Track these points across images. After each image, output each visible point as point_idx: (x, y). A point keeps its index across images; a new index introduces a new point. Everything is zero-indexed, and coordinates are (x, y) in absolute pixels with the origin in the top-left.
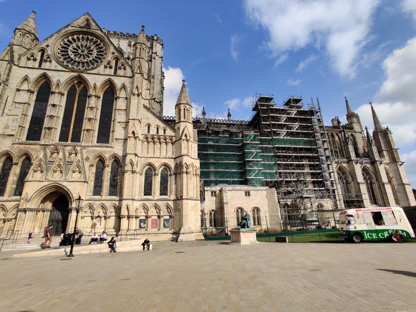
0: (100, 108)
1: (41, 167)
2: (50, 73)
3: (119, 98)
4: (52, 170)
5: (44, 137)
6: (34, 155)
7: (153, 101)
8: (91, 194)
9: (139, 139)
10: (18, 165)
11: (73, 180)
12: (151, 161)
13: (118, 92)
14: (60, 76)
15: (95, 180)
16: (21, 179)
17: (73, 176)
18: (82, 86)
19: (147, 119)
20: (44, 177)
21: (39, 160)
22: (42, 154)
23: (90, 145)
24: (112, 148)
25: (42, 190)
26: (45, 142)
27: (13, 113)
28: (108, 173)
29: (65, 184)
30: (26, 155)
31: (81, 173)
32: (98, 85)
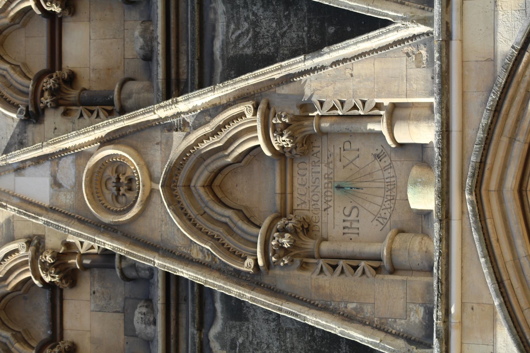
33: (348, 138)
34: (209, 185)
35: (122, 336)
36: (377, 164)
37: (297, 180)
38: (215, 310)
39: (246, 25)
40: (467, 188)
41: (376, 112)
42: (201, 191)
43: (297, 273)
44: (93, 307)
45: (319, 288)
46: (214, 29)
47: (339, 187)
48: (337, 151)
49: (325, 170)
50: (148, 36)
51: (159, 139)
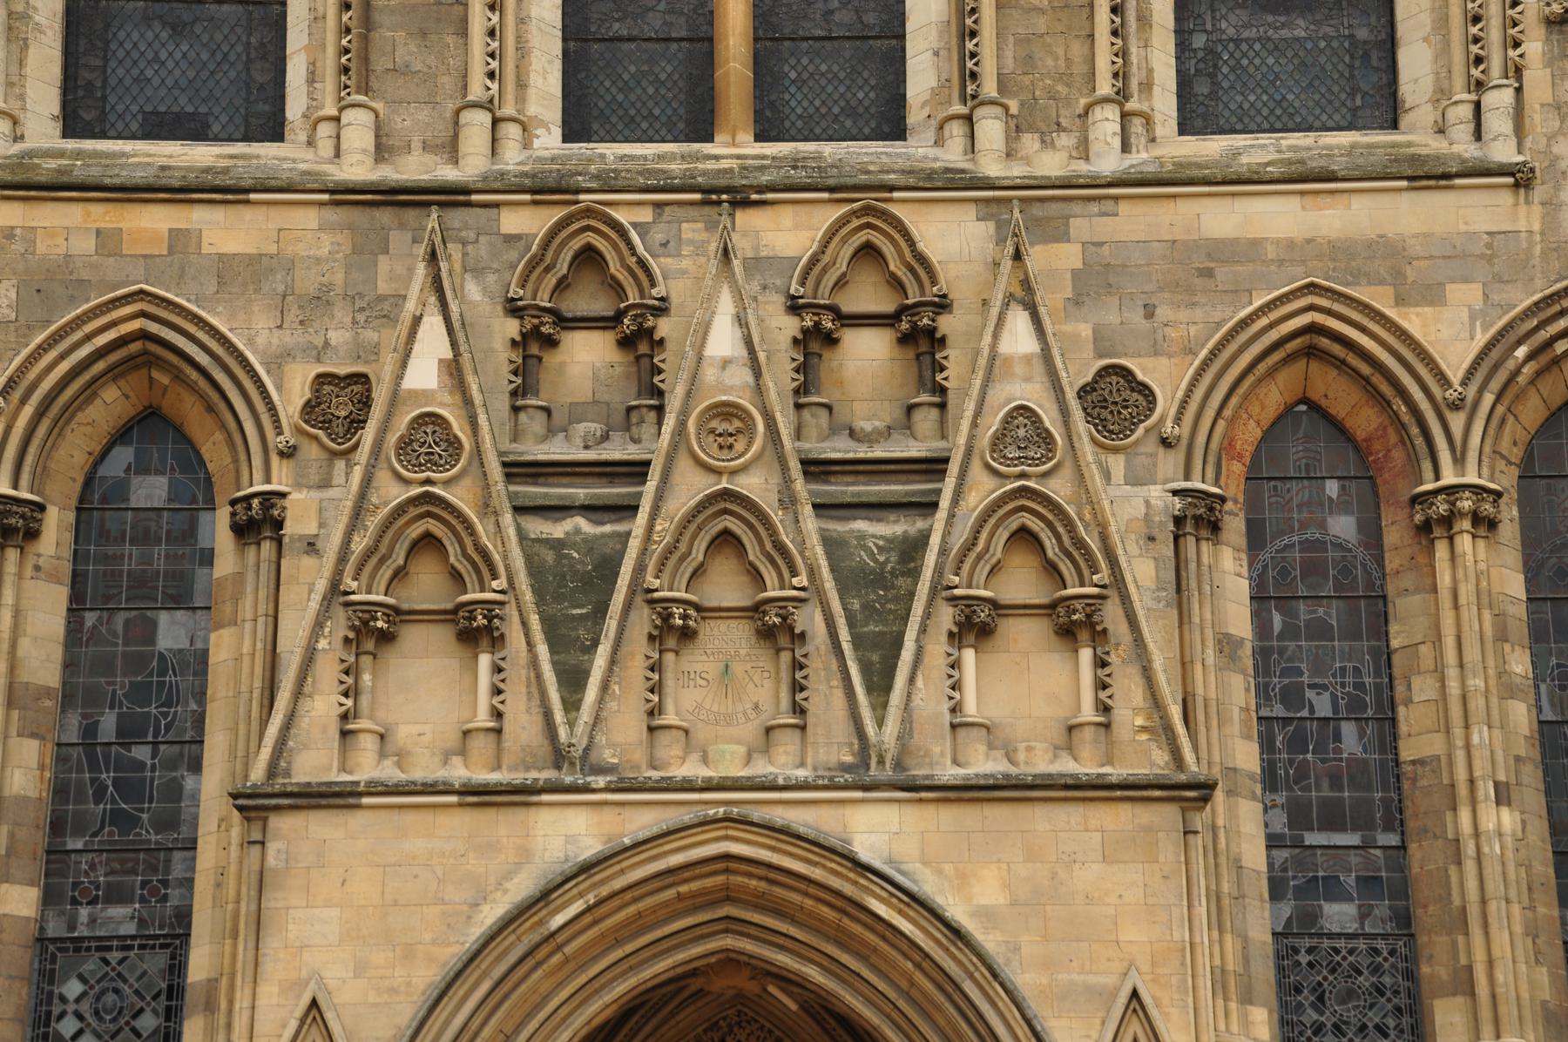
1: (453, 550)
4: (628, 607)
5: (365, 60)
6: (277, 362)
10: (32, 534)
11: (983, 764)
15: (1270, 780)
16: (107, 777)
17: (971, 709)
20: (523, 726)
21: (405, 445)
22: (432, 344)
23: (1108, 162)
24: (1520, 179)
26: (382, 150)
28: (1502, 636)
30: (136, 379)
31: (1099, 636)
33: (773, 675)
34: (726, 532)
35: (569, 400)
36: (749, 706)
37: (733, 623)
38: (603, 523)
39: (882, 559)
40: (729, 809)
41: (798, 709)
42: (720, 527)
43: (646, 631)
44: (598, 364)
45: (633, 654)
46: (879, 520)
47: (727, 666)
48: (761, 664)
49: (743, 652)
50: (874, 437)
51: (770, 481)
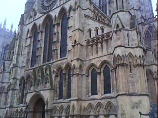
0: (60, 32)
2: (36, 22)
3: (69, 18)
7: (132, 10)
8: (57, 98)
9: (81, 45)
12: (93, 62)
13: (68, 14)
14: (40, 20)
18: (50, 22)
19: (89, 25)
23: (55, 61)
25: (32, 98)
27: (25, 53)
29: (42, 92)
32: (57, 15)
